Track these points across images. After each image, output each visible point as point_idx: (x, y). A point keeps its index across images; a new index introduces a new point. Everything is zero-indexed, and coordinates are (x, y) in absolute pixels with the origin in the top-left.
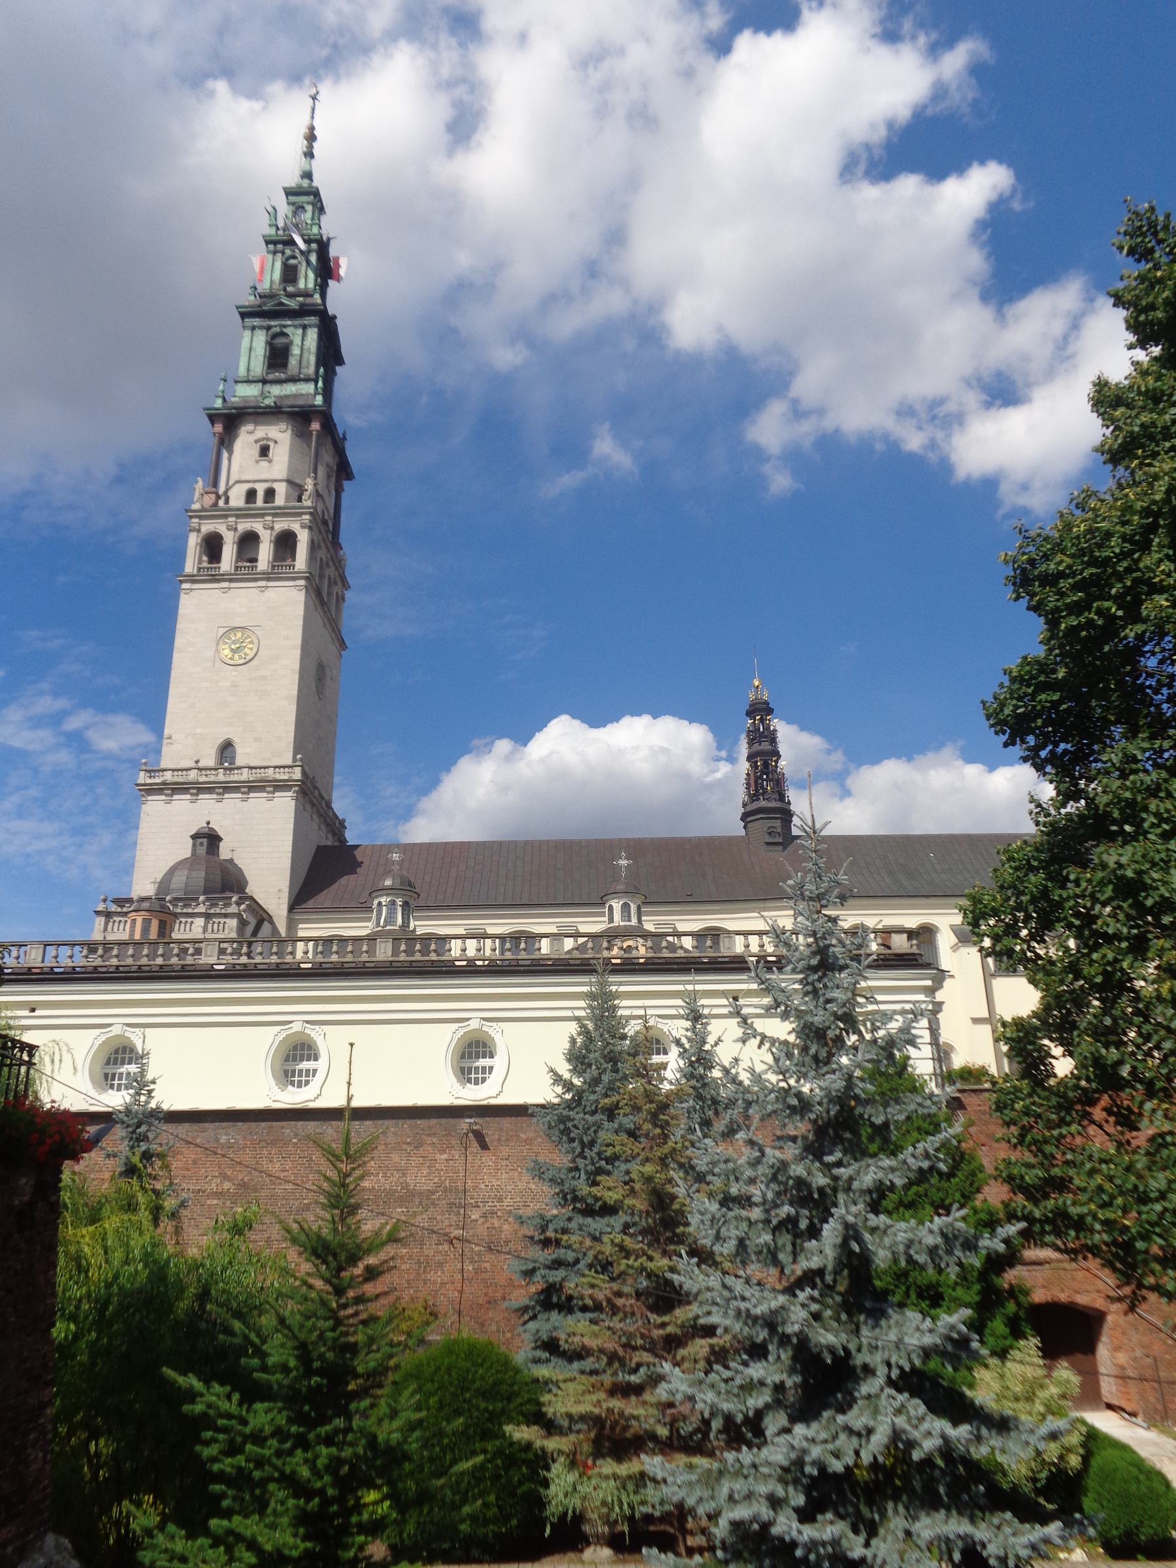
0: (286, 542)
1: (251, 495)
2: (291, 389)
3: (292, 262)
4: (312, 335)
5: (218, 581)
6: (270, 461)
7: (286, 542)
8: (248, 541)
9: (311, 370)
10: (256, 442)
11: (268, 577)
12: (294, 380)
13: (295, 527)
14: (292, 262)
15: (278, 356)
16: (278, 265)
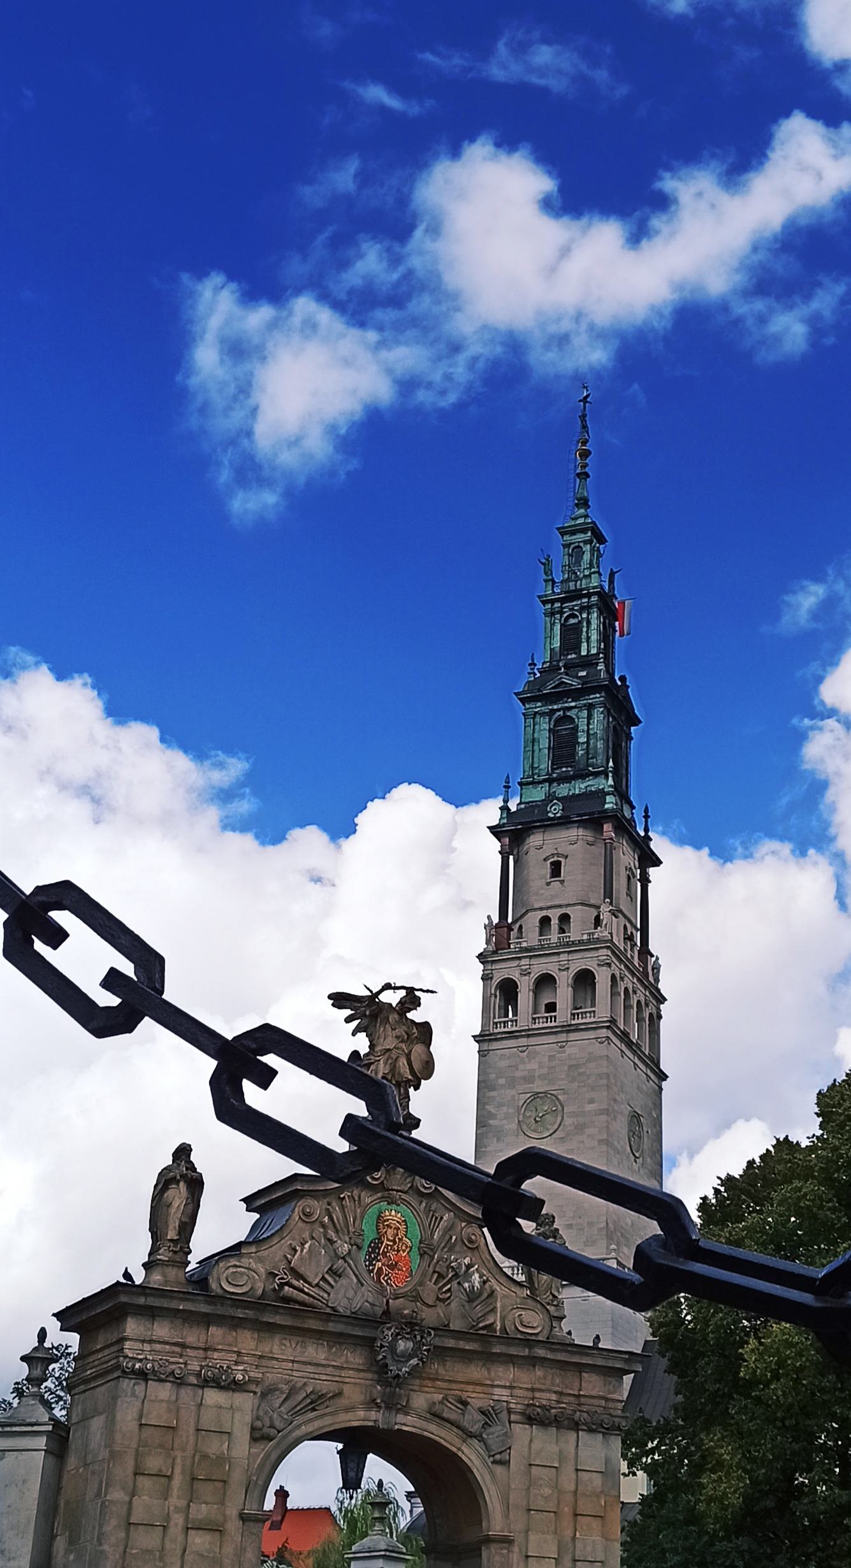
0: (585, 980)
1: (545, 922)
2: (579, 787)
3: (572, 621)
4: (598, 715)
5: (517, 1037)
6: (562, 882)
7: (585, 980)
8: (546, 981)
9: (600, 760)
10: (545, 860)
11: (569, 1029)
12: (582, 775)
13: (591, 965)
14: (572, 621)
15: (563, 746)
16: (557, 628)
